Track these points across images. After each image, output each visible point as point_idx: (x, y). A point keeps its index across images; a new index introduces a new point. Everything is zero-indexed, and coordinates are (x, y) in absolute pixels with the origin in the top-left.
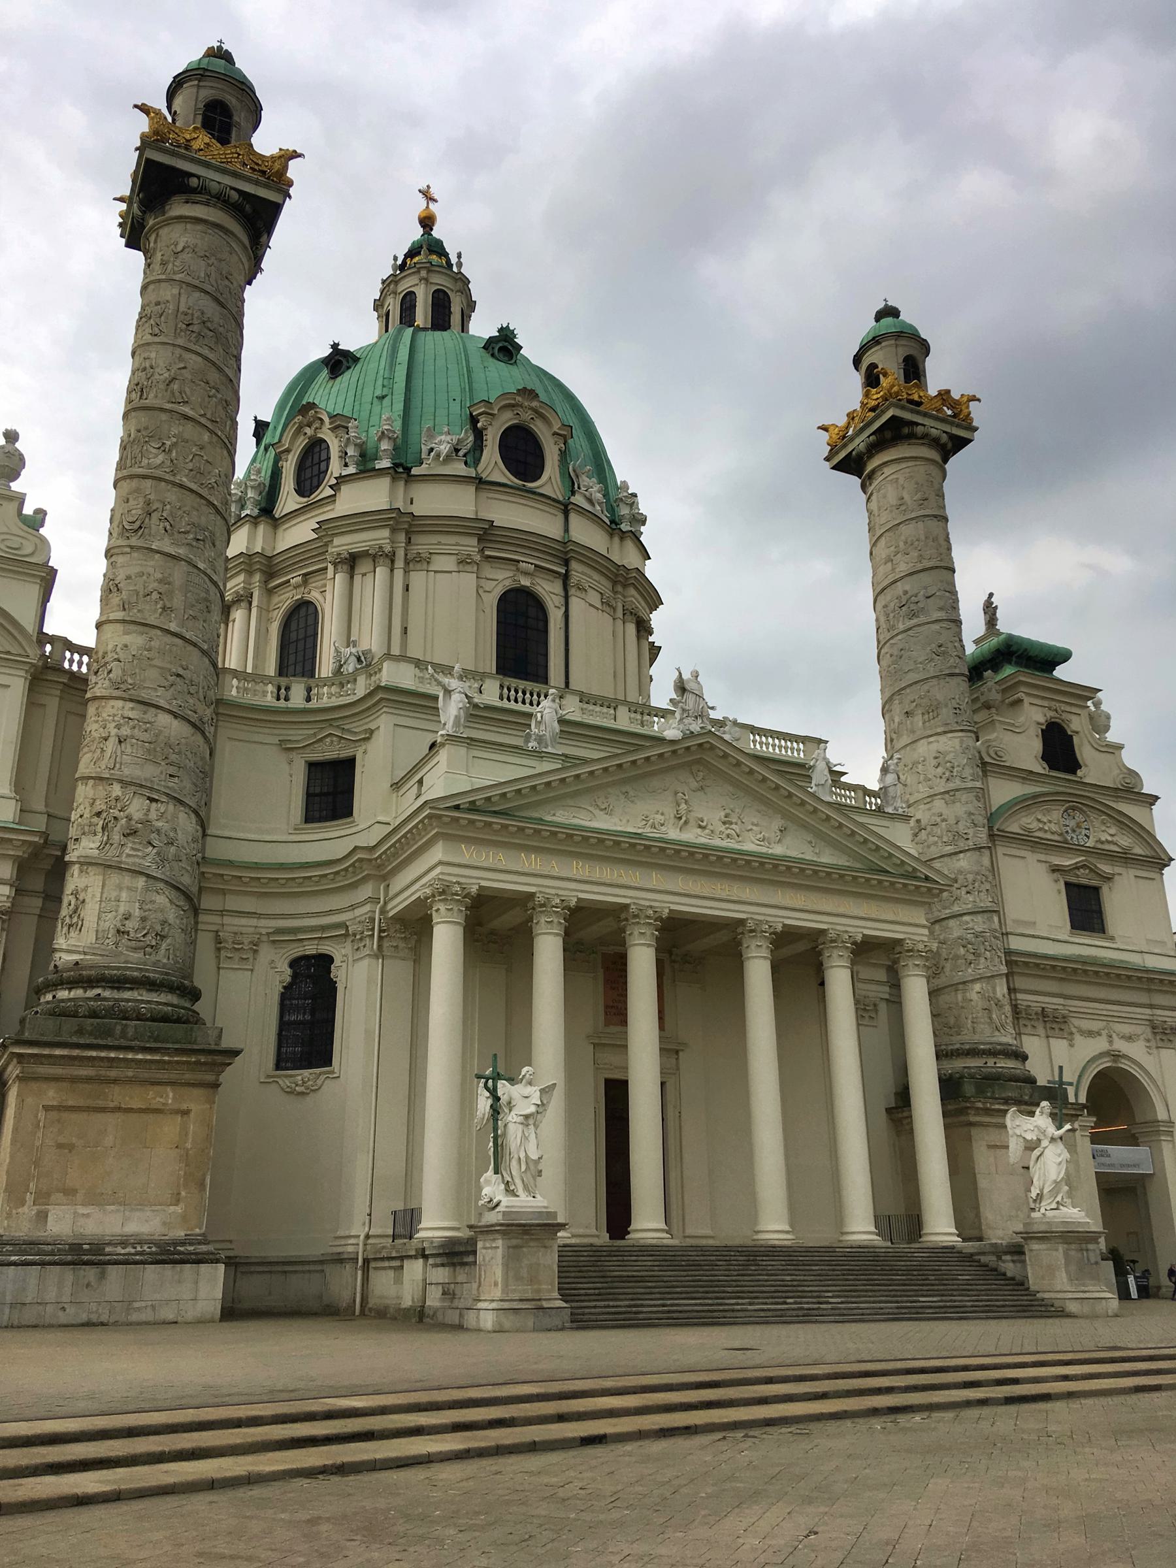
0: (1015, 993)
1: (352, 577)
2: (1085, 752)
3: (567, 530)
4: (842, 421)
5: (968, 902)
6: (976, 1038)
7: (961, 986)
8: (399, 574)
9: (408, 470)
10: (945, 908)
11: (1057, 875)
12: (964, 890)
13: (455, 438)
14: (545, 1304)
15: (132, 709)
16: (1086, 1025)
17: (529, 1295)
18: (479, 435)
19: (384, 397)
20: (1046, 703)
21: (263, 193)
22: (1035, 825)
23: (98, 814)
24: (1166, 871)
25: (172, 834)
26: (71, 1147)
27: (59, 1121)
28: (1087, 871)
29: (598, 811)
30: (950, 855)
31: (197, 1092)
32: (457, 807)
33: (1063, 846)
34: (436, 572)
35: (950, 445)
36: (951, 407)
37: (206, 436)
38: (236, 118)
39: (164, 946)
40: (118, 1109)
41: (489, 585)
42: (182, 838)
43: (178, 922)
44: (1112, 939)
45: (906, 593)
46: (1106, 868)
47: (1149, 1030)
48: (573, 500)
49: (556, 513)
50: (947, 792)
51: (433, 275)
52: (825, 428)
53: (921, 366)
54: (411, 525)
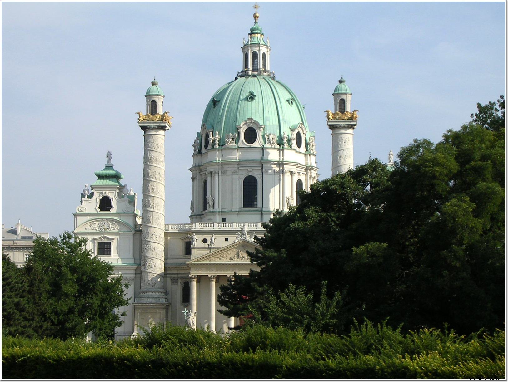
1: (211, 177)
3: (263, 155)
8: (220, 177)
9: (222, 146)
18: (239, 134)
19: (218, 122)
21: (162, 125)
26: (143, 319)
34: (228, 175)
35: (350, 126)
37: (155, 183)
38: (157, 103)
39: (156, 284)
40: (150, 312)
41: (241, 176)
49: (259, 150)
53: (346, 100)
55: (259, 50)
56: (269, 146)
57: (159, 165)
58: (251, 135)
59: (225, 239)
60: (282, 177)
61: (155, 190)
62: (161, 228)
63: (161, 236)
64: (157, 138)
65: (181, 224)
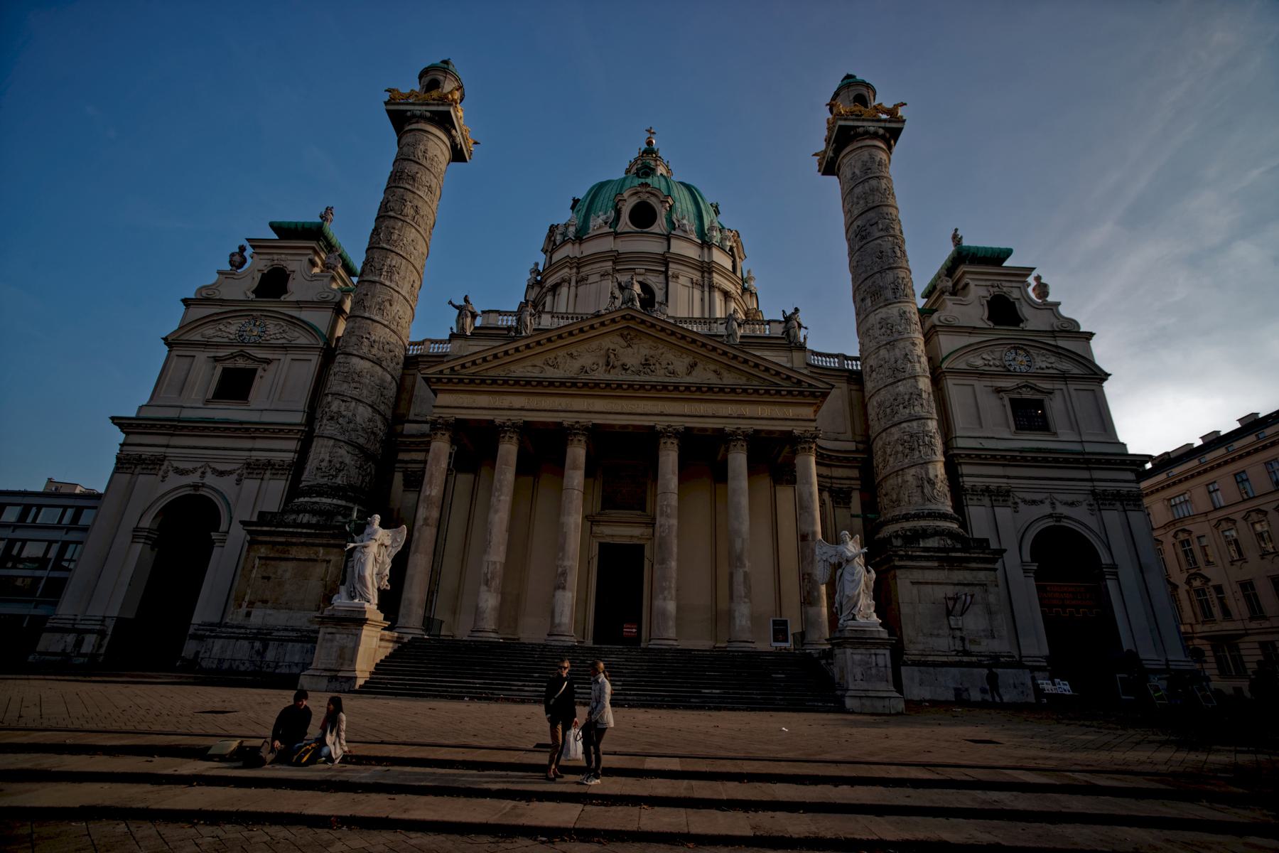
1: (554, 296)
2: (1025, 311)
3: (669, 247)
4: (822, 146)
7: (900, 472)
8: (573, 289)
10: (889, 421)
11: (1002, 394)
12: (901, 406)
13: (604, 217)
14: (340, 674)
16: (1028, 497)
17: (333, 667)
20: (989, 283)
21: (441, 108)
22: (979, 362)
24: (1105, 384)
25: (351, 417)
26: (268, 578)
27: (265, 564)
28: (1029, 389)
29: (547, 368)
30: (891, 384)
31: (335, 550)
32: (441, 372)
33: (1007, 373)
35: (888, 135)
36: (884, 112)
37: (400, 224)
38: (442, 84)
39: (341, 474)
42: (358, 419)
43: (353, 463)
44: (1055, 434)
45: (858, 226)
46: (1046, 385)
47: (1091, 497)
48: (673, 232)
50: (886, 344)
52: (816, 155)
54: (578, 264)
56: (681, 234)
57: (418, 189)
58: (643, 216)
60: (706, 294)
61: (395, 237)
62: (392, 327)
64: (425, 139)
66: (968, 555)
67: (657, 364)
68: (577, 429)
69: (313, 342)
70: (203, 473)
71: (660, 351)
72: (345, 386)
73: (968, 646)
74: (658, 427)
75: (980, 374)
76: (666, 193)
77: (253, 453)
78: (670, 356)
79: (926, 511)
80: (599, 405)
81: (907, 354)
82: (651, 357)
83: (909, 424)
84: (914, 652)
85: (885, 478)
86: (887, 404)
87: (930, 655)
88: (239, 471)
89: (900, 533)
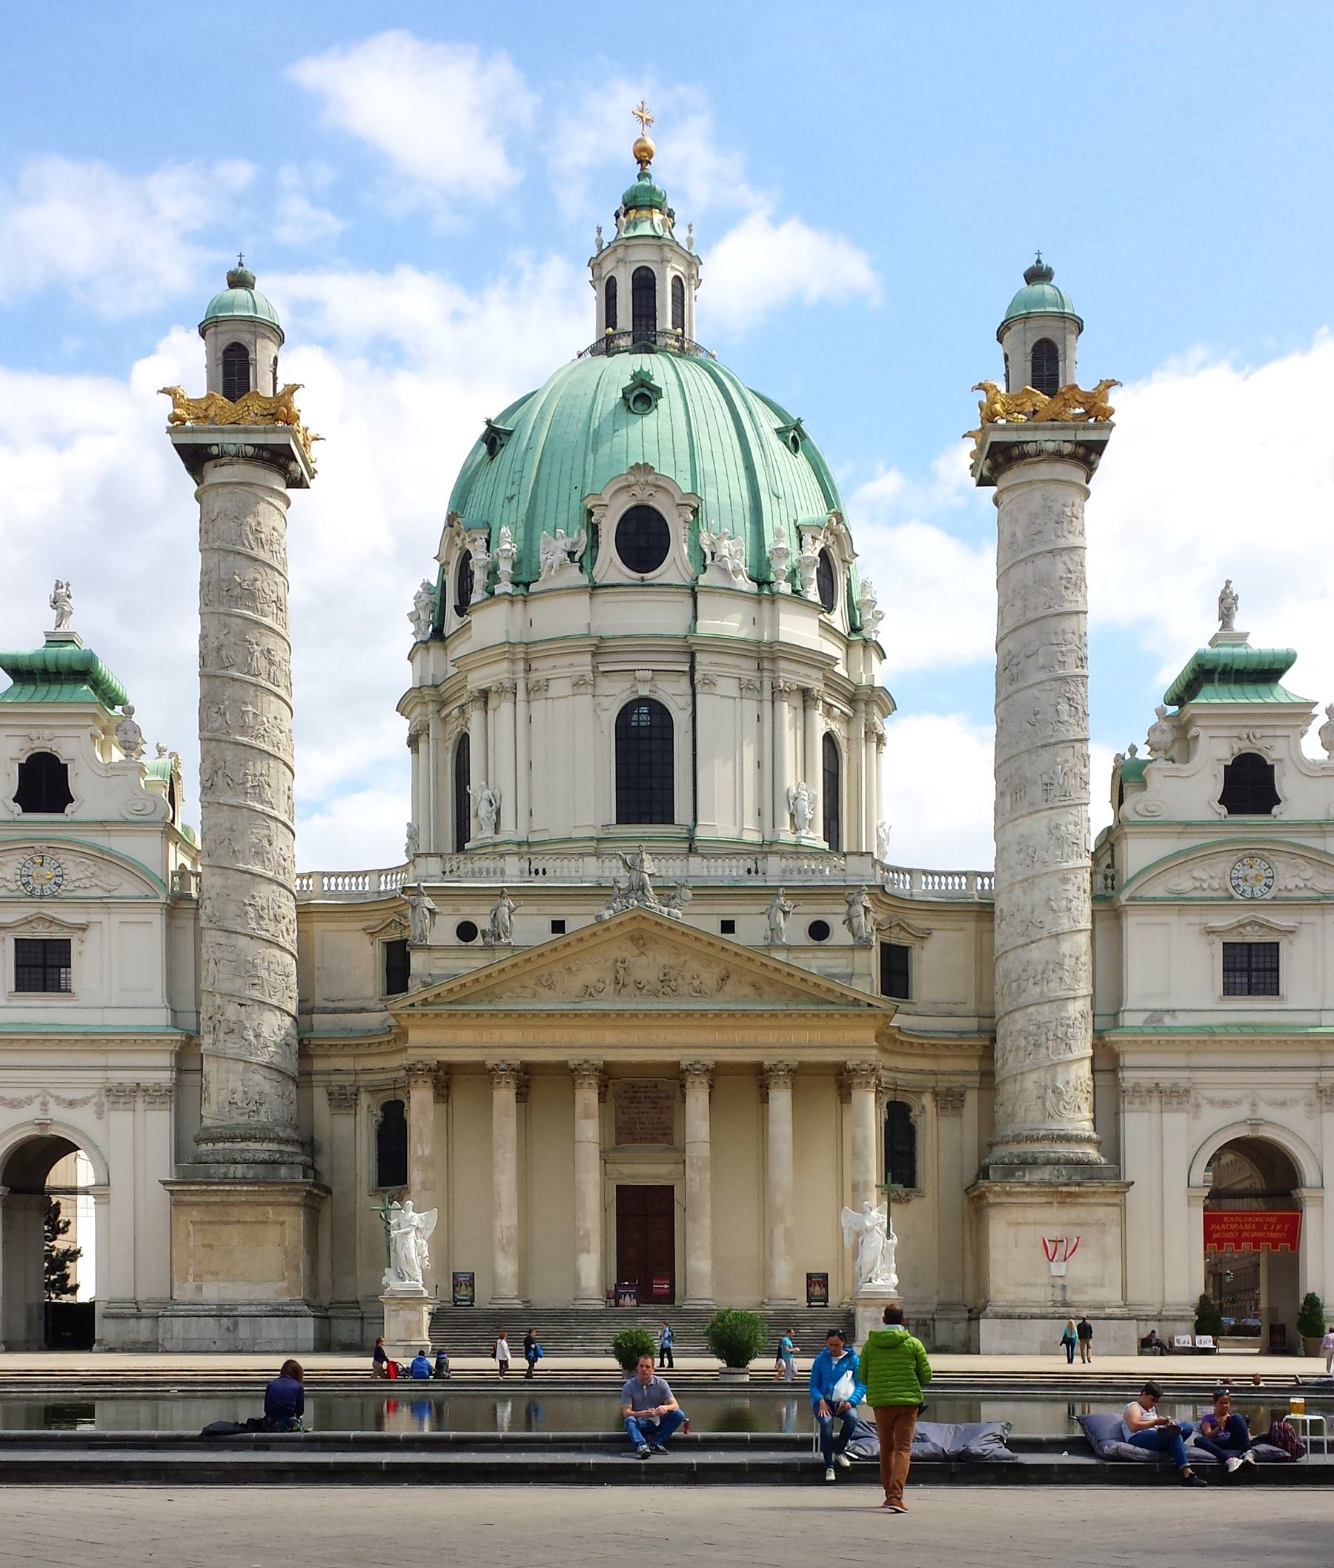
0: (1123, 1071)
5: (1034, 992)
6: (1028, 1125)
7: (1019, 1077)
12: (1031, 981)
15: (221, 936)
23: (211, 1018)
29: (543, 989)
30: (1022, 946)
51: (631, 250)
55: (664, 261)
59: (553, 922)
62: (281, 878)
63: (284, 911)
65: (365, 874)
66: (1083, 1189)
67: (680, 980)
68: (586, 1070)
69: (147, 891)
70: (44, 1104)
71: (682, 959)
72: (238, 983)
73: (1070, 1296)
74: (683, 1066)
75: (1180, 902)
76: (687, 488)
77: (110, 1074)
78: (694, 966)
79: (1042, 1133)
80: (610, 1037)
81: (1050, 899)
82: (671, 968)
83: (1039, 1008)
84: (1001, 1303)
85: (1003, 1081)
86: (1014, 976)
87: (1019, 1307)
88: (95, 1100)
89: (1006, 1160)
